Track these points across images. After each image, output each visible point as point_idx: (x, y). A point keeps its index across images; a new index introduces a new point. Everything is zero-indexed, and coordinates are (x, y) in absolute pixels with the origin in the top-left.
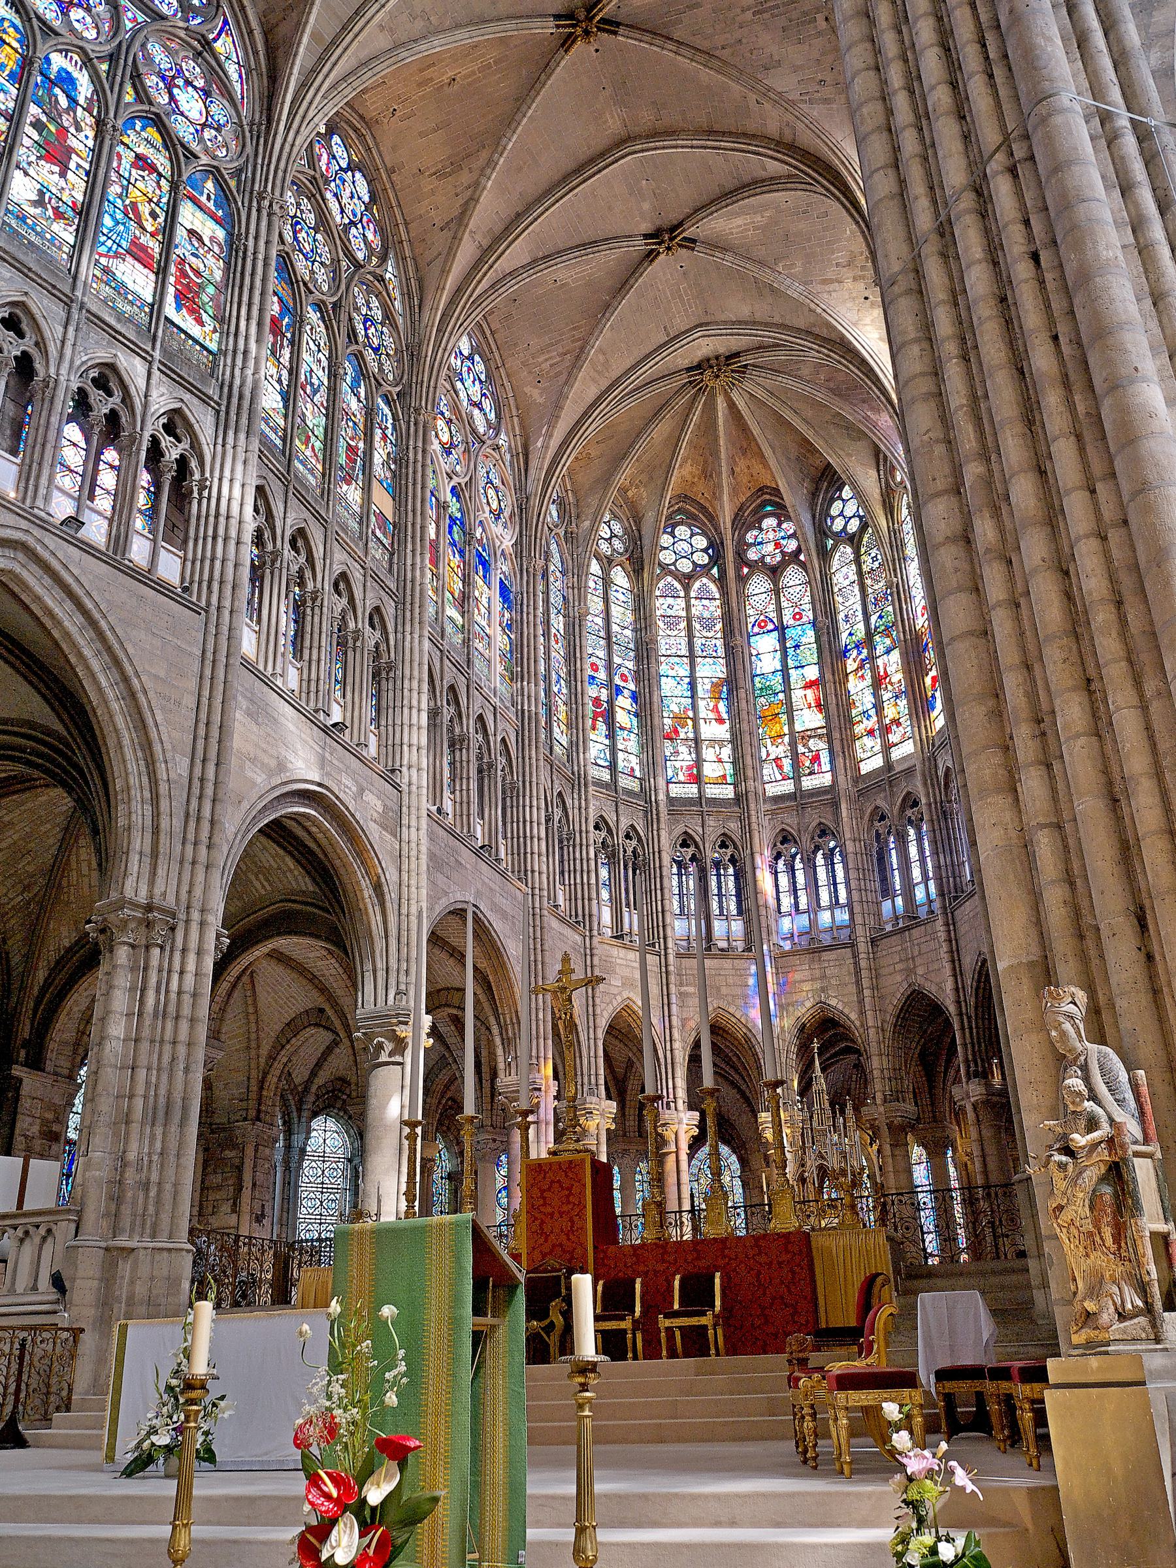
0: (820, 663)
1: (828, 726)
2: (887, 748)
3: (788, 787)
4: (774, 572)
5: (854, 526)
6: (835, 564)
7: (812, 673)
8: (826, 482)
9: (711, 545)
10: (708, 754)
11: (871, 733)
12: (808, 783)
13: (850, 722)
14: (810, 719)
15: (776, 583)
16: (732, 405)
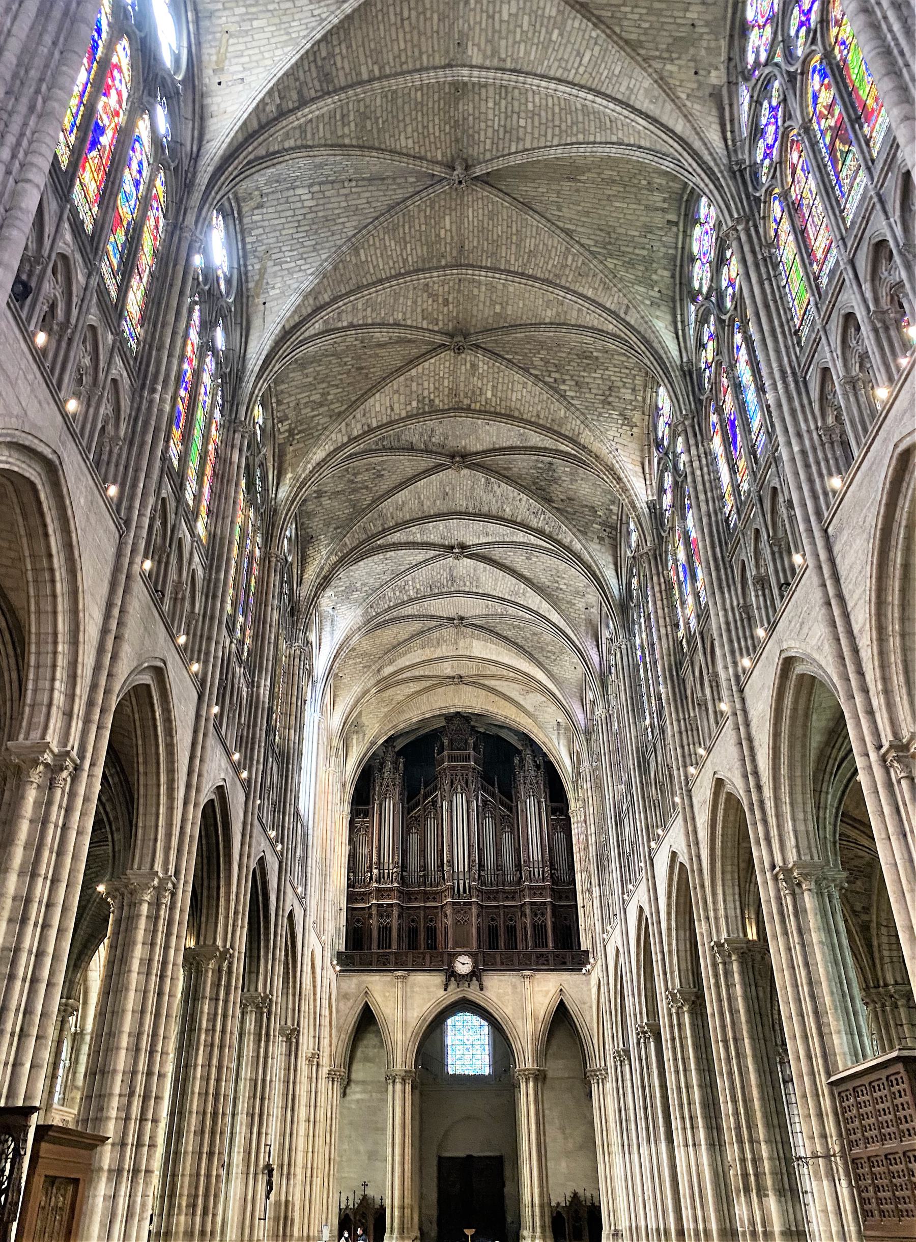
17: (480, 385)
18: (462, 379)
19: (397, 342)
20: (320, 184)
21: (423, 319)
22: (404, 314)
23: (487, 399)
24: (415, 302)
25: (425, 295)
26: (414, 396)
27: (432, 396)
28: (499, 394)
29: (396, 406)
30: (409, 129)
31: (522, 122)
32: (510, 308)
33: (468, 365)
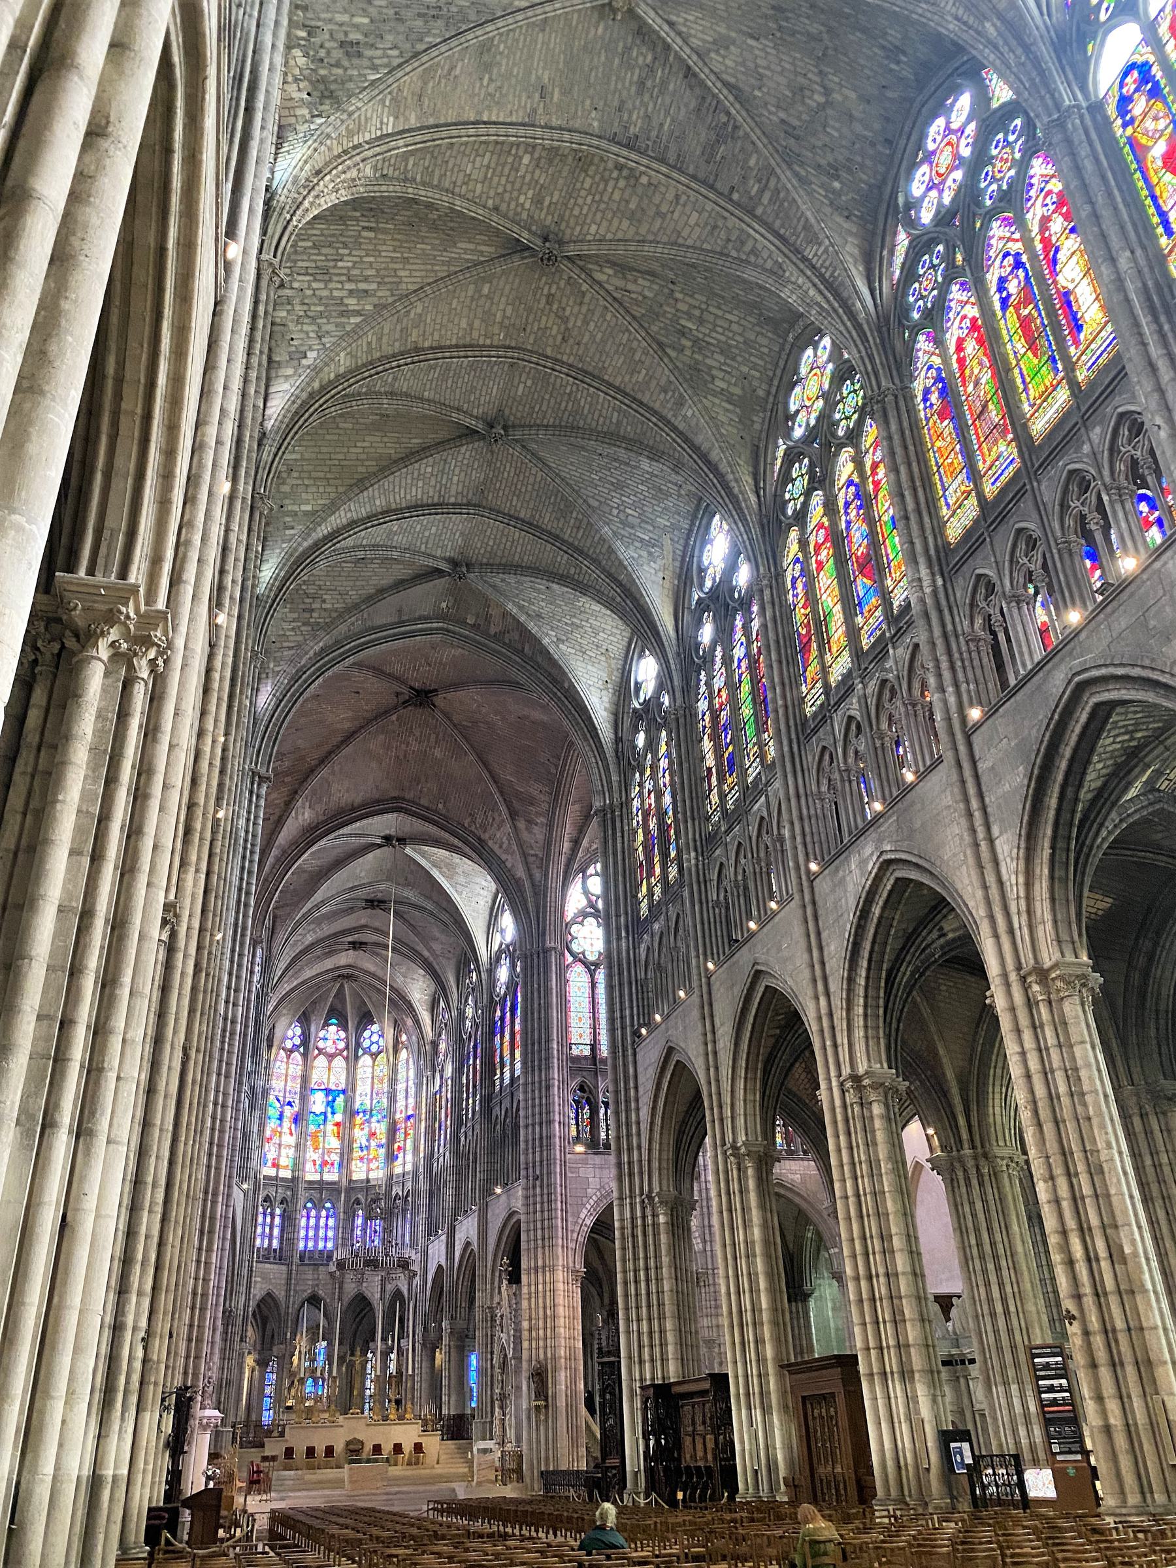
0: (345, 1112)
1: (342, 1149)
2: (368, 1170)
3: (317, 1177)
4: (331, 1057)
5: (374, 1048)
6: (361, 1062)
7: (339, 1117)
8: (366, 1019)
9: (303, 1033)
10: (284, 1152)
11: (362, 1159)
12: (327, 1177)
13: (351, 1150)
14: (334, 1143)
15: (330, 1062)
16: (342, 985)
17: (538, 172)
18: (561, 181)
19: (632, 269)
20: (628, 464)
21: (584, 294)
22: (603, 316)
23: (532, 154)
24: (586, 322)
25: (570, 325)
26: (640, 190)
27: (615, 174)
28: (510, 160)
29: (670, 196)
30: (531, 480)
31: (429, 469)
32: (470, 293)
33: (546, 203)
